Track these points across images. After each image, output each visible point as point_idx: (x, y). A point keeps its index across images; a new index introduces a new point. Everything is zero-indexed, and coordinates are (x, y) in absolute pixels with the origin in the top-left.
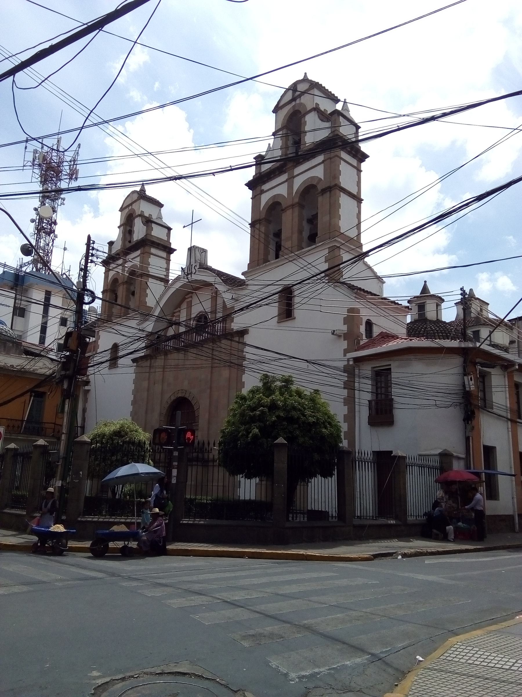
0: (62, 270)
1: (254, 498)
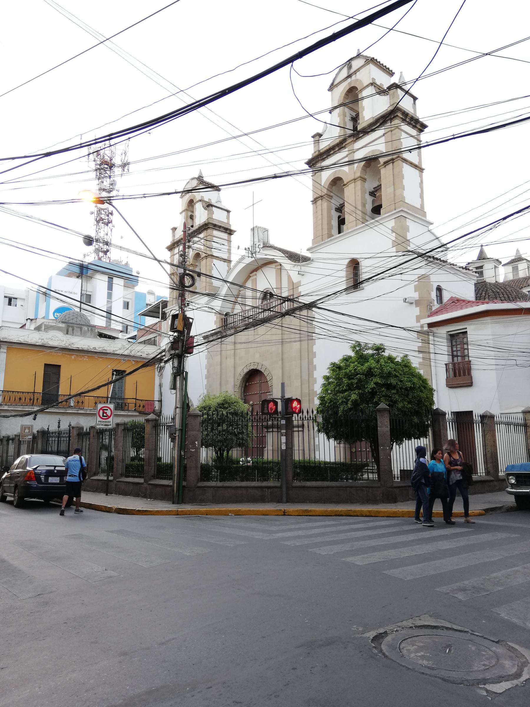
1: (334, 461)
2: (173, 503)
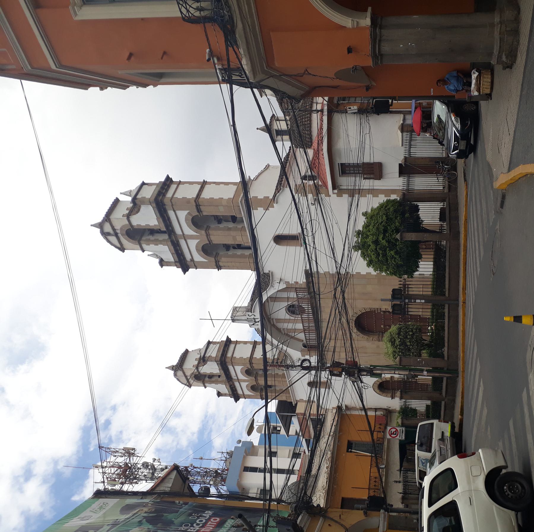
0: (222, 460)
2: (458, 377)
